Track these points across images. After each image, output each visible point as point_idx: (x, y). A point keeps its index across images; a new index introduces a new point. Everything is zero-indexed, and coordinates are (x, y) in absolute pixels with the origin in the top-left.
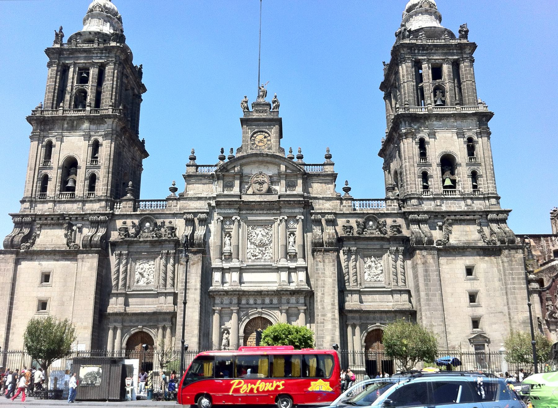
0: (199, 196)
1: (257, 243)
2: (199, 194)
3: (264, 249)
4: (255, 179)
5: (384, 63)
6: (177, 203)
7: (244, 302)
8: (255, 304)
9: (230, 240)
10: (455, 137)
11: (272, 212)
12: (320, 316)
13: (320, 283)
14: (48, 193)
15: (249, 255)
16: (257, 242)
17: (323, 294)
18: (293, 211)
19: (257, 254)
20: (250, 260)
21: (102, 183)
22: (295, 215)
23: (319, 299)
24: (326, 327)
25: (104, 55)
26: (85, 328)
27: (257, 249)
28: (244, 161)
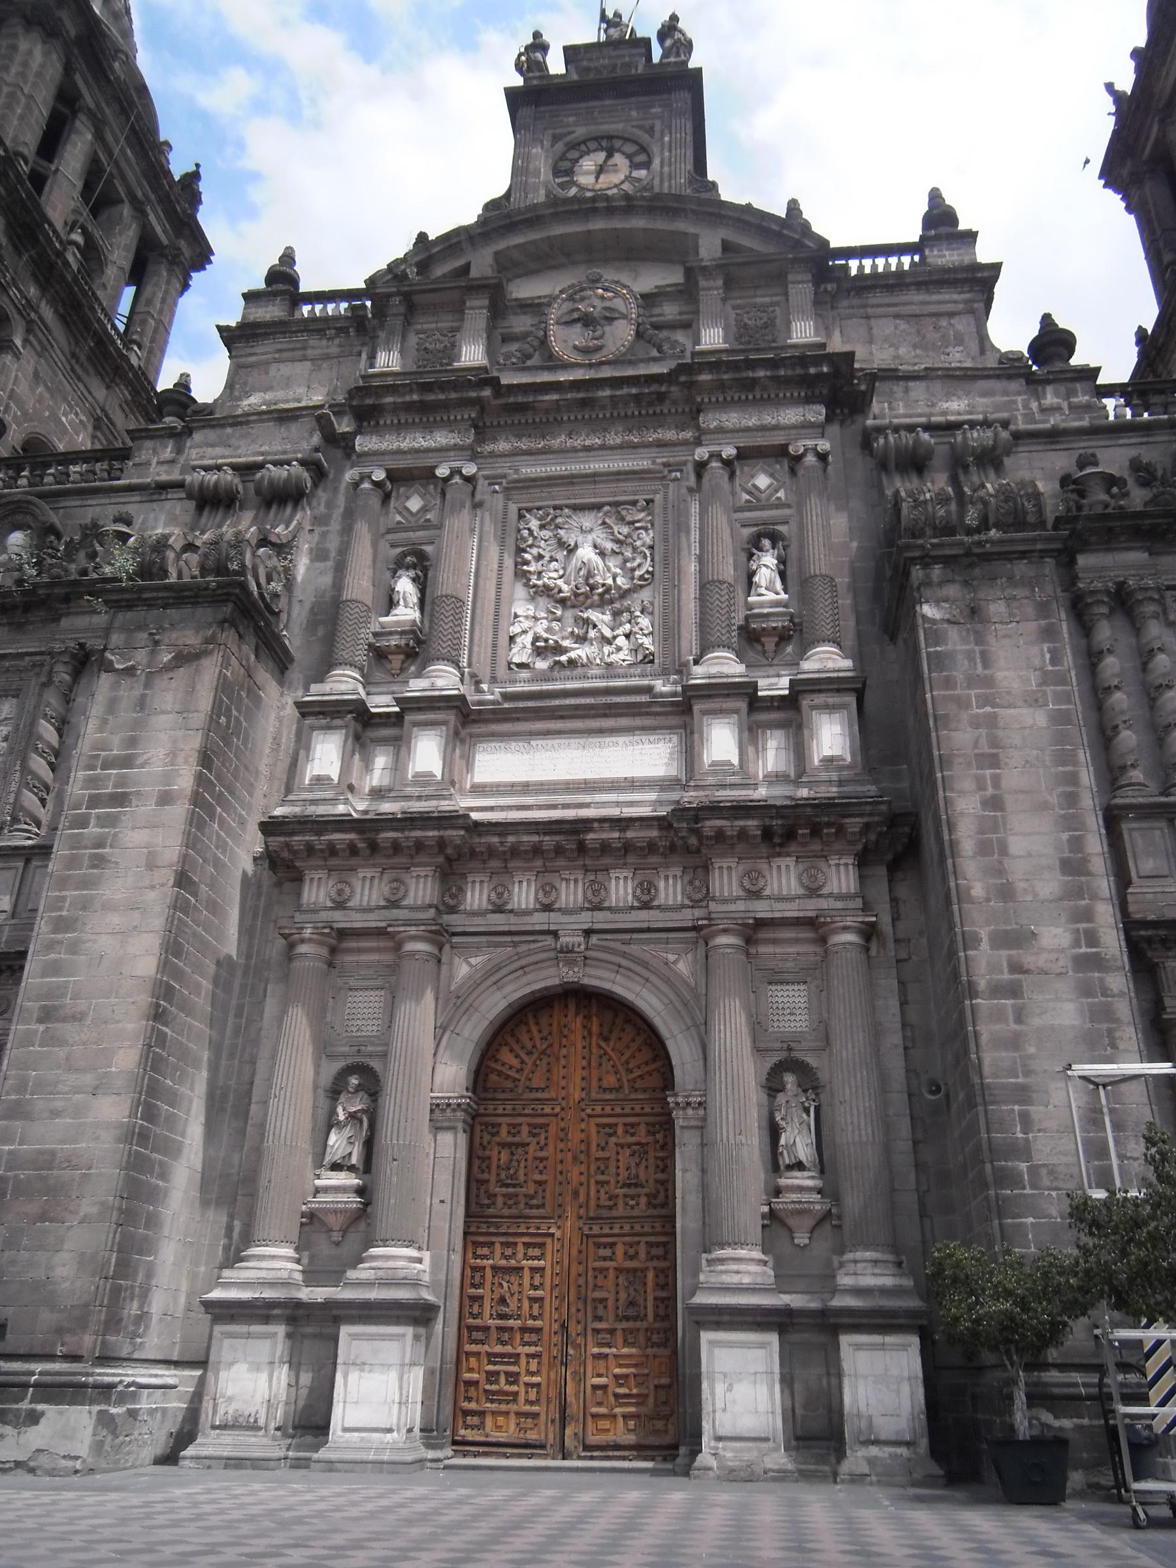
2: (287, 401)
3: (607, 618)
6: (179, 450)
7: (476, 896)
8: (547, 908)
9: (422, 584)
11: (651, 437)
12: (985, 945)
16: (565, 588)
17: (995, 803)
18: (768, 419)
19: (566, 643)
20: (525, 674)
22: (778, 439)
24: (1037, 1022)
27: (569, 614)
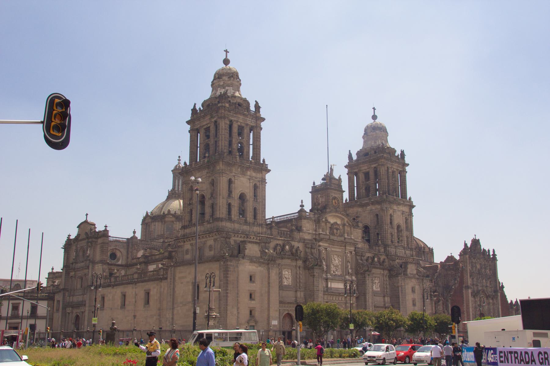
0: (308, 232)
1: (335, 265)
4: (335, 227)
5: (350, 151)
10: (402, 216)
13: (367, 291)
14: (233, 216)
15: (332, 272)
17: (369, 297)
21: (261, 215)
22: (351, 251)
23: (367, 300)
25: (253, 120)
26: (276, 311)
27: (335, 267)
28: (331, 214)
